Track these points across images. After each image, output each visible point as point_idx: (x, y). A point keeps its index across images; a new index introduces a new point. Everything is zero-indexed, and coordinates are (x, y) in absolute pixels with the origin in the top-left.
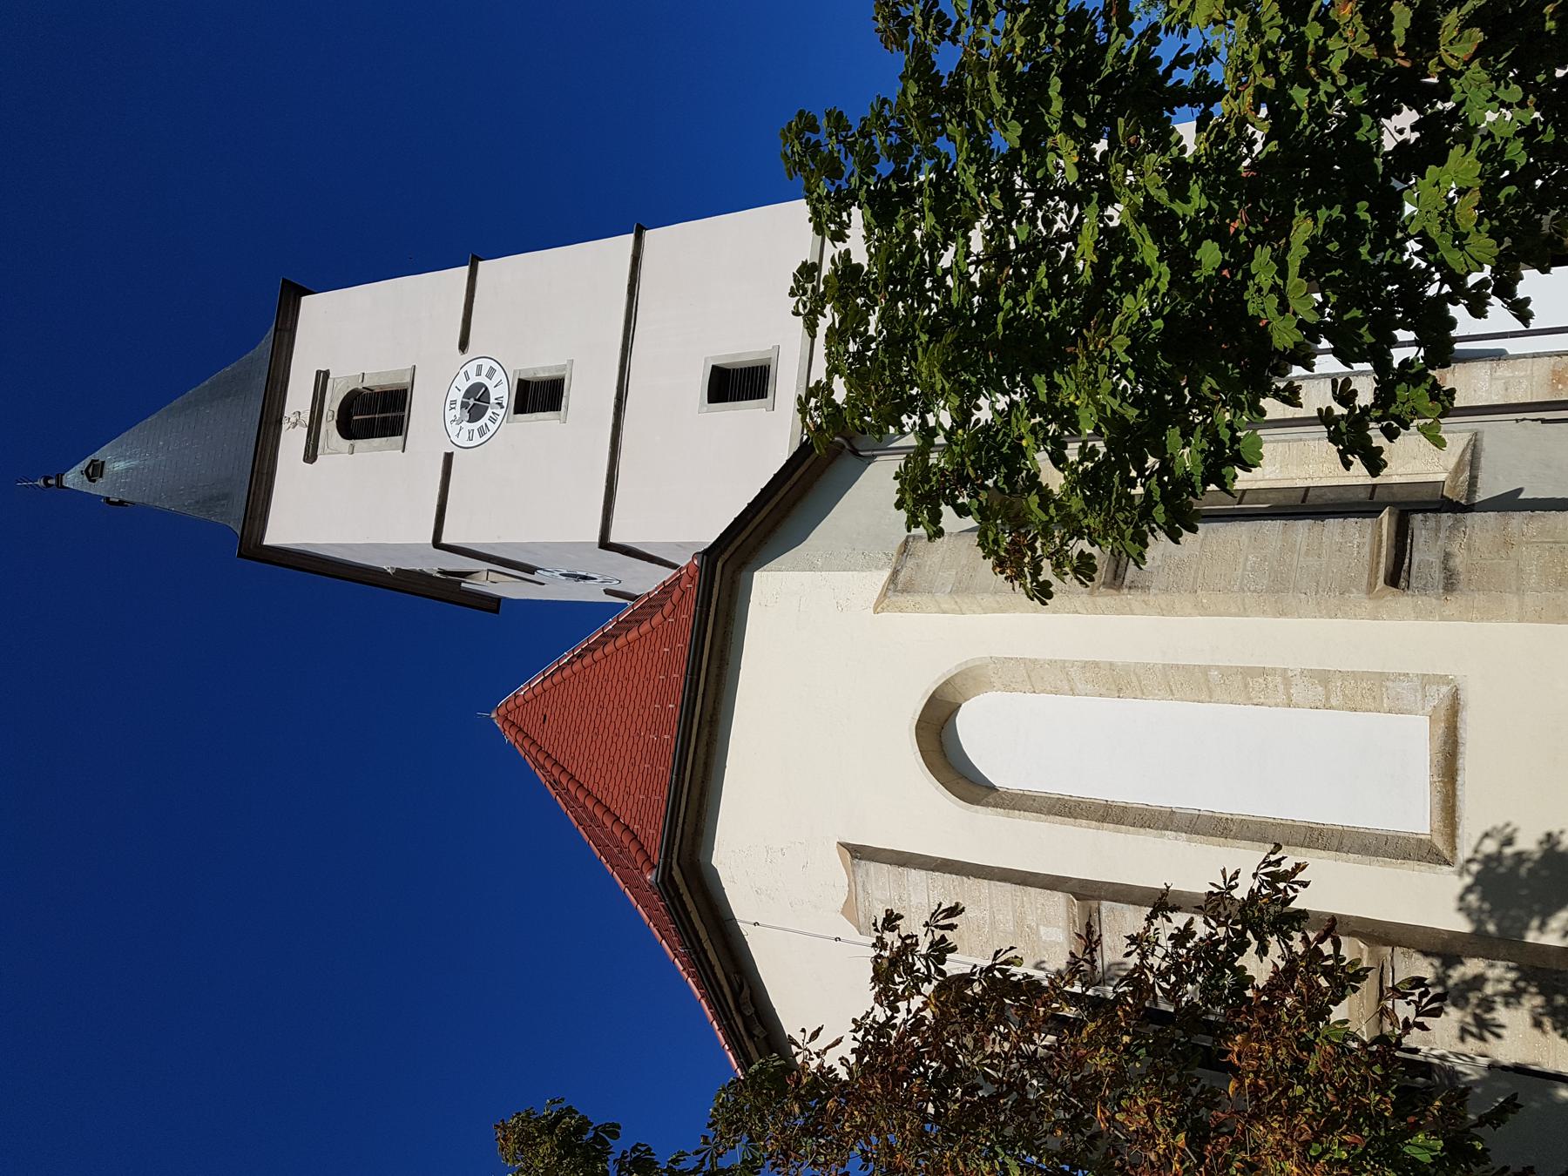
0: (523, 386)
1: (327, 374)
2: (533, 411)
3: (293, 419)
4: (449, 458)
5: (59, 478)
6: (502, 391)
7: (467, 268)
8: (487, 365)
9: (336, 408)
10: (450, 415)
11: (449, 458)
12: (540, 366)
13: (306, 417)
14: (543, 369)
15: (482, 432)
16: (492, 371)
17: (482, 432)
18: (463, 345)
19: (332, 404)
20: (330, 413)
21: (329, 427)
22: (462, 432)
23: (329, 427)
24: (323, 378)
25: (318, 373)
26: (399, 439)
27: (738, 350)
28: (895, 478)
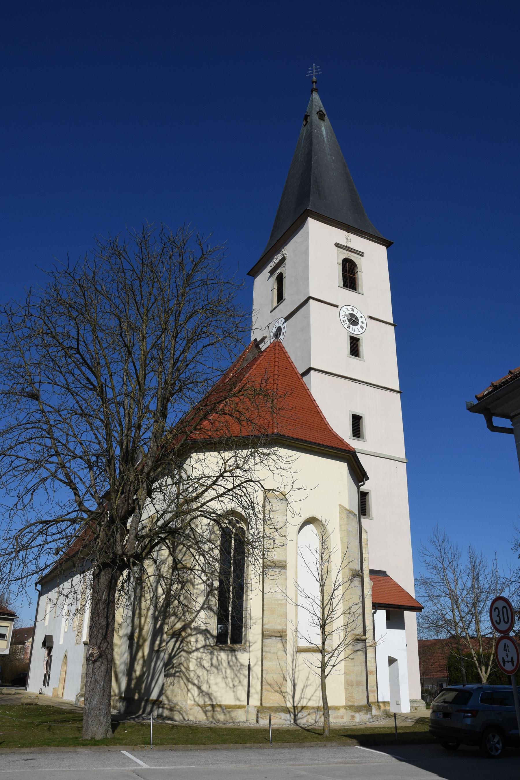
0: (358, 340)
1: (363, 256)
2: (351, 343)
3: (349, 238)
4: (337, 306)
5: (316, 90)
6: (356, 331)
7: (392, 322)
8: (364, 326)
9: (352, 258)
10: (349, 308)
11: (337, 306)
12: (364, 347)
13: (349, 245)
14: (363, 349)
15: (344, 321)
16: (362, 328)
17: (344, 321)
18: (371, 317)
19: (353, 257)
20: (350, 256)
21: (346, 254)
22: (346, 311)
23: (346, 254)
24: (361, 254)
25: (364, 253)
26: (342, 285)
27: (367, 426)
28: (282, 566)
